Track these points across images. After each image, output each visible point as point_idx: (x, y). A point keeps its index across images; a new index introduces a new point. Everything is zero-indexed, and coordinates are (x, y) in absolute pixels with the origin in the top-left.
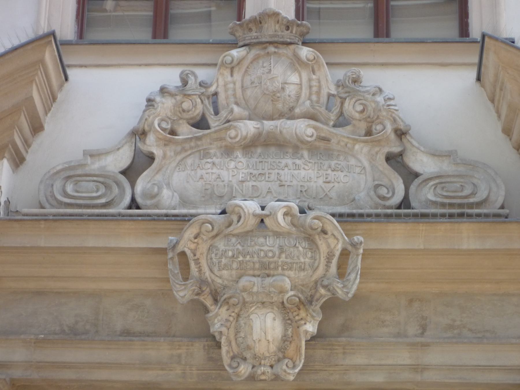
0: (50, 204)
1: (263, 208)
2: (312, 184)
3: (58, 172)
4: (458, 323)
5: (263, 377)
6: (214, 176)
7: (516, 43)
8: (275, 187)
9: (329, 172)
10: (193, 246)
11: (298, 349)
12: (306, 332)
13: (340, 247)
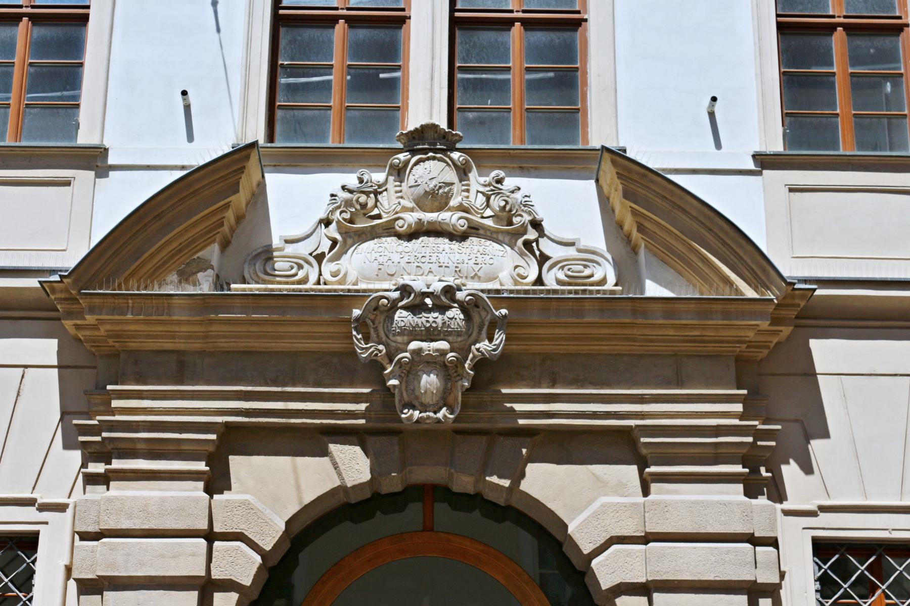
0: (378, 336)
1: (428, 286)
2: (465, 265)
3: (258, 255)
4: (581, 377)
5: (428, 421)
6: (386, 258)
7: (628, 151)
8: (434, 267)
9: (478, 255)
10: (372, 317)
11: (456, 399)
12: (463, 386)
13: (489, 317)
